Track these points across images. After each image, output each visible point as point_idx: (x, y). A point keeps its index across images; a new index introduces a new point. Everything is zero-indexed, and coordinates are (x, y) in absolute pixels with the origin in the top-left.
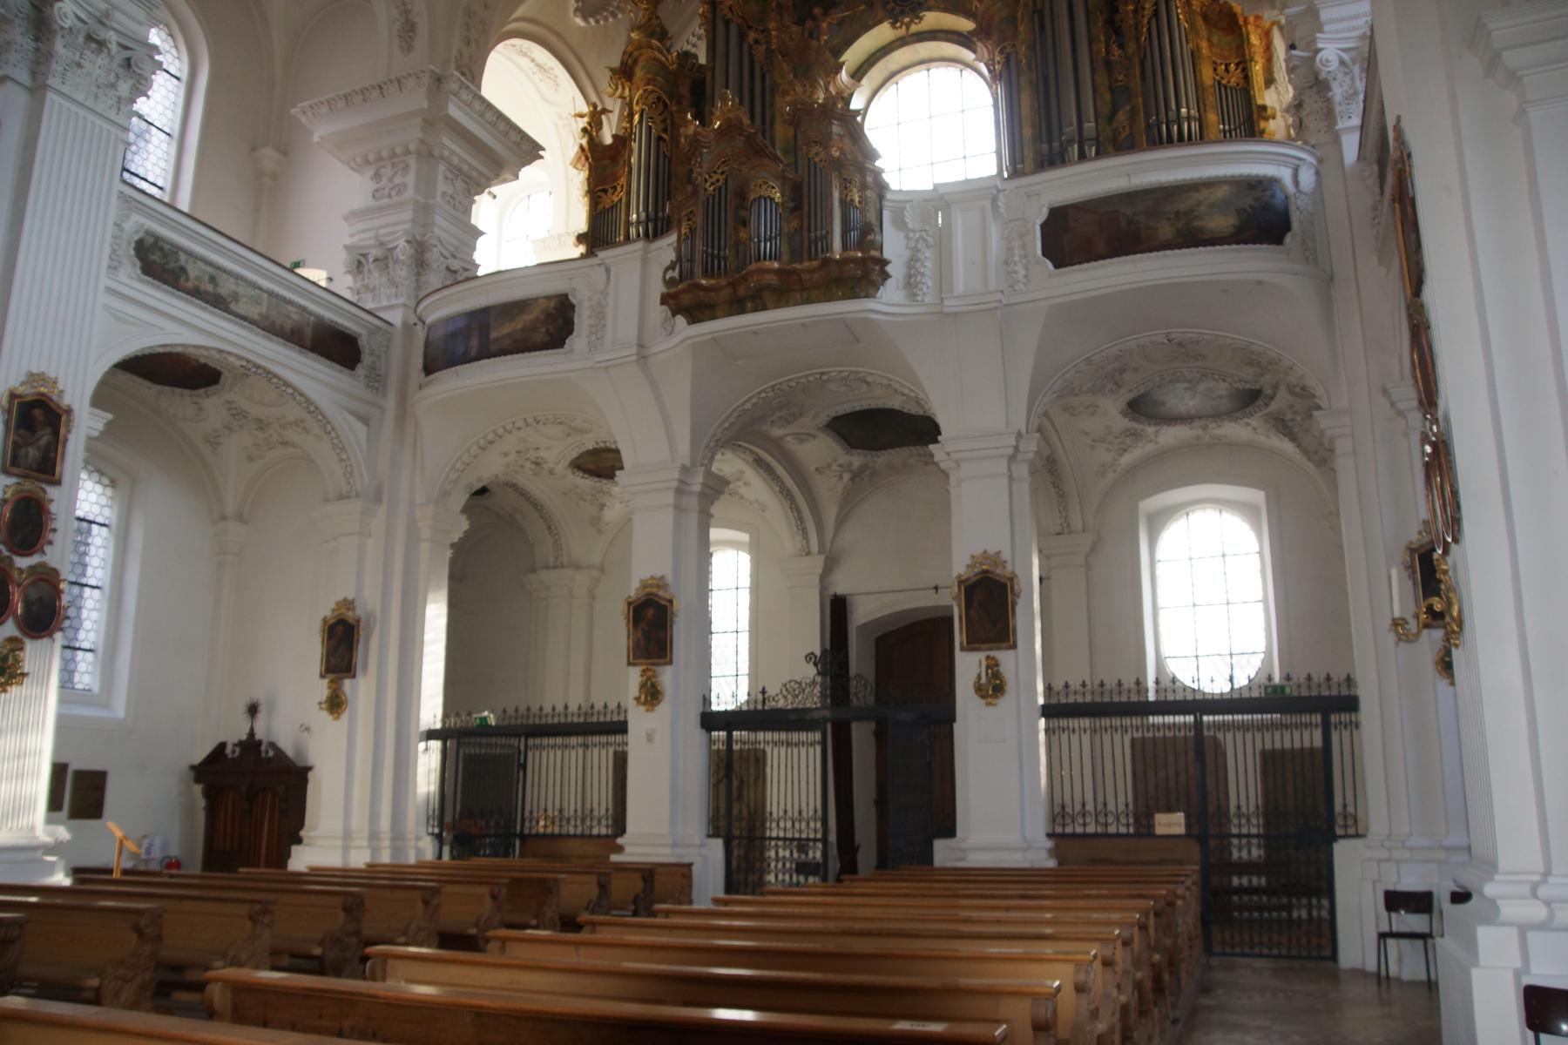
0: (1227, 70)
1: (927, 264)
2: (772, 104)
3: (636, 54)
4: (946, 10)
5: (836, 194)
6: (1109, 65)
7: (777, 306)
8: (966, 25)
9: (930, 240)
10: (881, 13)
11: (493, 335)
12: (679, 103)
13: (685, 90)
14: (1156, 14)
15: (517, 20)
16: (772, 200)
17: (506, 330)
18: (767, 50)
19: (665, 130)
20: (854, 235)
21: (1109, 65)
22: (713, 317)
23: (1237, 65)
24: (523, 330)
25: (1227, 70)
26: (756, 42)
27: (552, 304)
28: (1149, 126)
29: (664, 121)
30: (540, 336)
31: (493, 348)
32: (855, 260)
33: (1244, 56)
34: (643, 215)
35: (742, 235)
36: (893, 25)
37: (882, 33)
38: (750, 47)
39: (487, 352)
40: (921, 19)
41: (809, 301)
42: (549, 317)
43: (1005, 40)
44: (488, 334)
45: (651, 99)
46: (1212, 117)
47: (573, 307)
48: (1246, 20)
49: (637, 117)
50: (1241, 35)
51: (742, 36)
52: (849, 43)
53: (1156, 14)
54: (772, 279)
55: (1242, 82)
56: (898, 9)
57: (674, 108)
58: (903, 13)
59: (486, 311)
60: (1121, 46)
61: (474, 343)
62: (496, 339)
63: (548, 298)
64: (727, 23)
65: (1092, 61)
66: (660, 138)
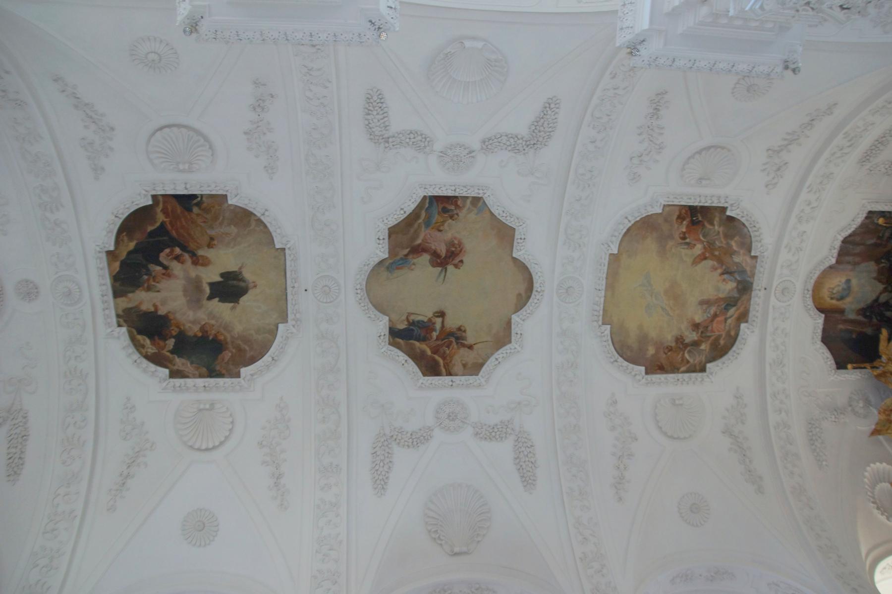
15: (867, 554)
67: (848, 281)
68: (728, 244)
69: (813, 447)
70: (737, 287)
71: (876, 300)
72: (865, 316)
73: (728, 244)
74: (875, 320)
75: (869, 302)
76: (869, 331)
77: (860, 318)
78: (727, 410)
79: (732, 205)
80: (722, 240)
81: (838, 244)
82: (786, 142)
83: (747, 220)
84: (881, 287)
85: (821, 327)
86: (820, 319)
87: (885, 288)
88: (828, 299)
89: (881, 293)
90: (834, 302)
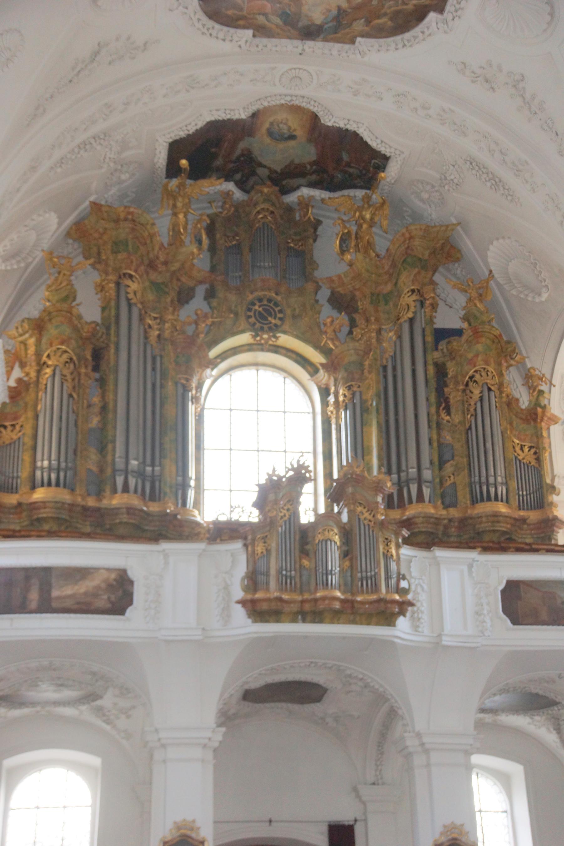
0: (522, 449)
1: (425, 604)
2: (162, 386)
3: (54, 314)
4: (297, 337)
5: (381, 547)
6: (439, 426)
7: (332, 622)
8: (317, 358)
9: (425, 587)
10: (243, 323)
11: (55, 593)
12: (86, 367)
13: (88, 355)
14: (481, 399)
16: (335, 543)
17: (68, 591)
18: (159, 336)
19: (74, 388)
20: (393, 581)
21: (439, 426)
22: (278, 621)
23: (531, 448)
24: (86, 594)
25: (522, 449)
26: (150, 327)
27: (113, 576)
28: (471, 484)
29: (73, 379)
30: (102, 602)
31: (54, 605)
32: (394, 602)
33: (538, 443)
34: (54, 463)
35: (305, 562)
36: (254, 337)
37: (245, 338)
38: (145, 329)
39: (46, 606)
40: (277, 338)
41: (353, 622)
42: (110, 587)
43: (353, 380)
44: (49, 592)
45: (65, 357)
46: (513, 484)
47: (132, 583)
48: (542, 420)
49: (48, 371)
50: (536, 427)
51: (141, 319)
52: (215, 342)
53: (481, 399)
54: (337, 605)
55: (533, 463)
56: (258, 325)
57: (83, 370)
58: (262, 329)
59: (47, 570)
60: (449, 413)
61: (34, 596)
62: (58, 598)
63: (108, 570)
64: (130, 305)
65: (429, 421)
66: (70, 396)
67: (292, 137)
68: (385, 14)
69: (76, 150)
70: (313, 24)
71: (260, 165)
72: (240, 156)
73: (385, 14)
74: (231, 165)
75: (260, 159)
76: (219, 162)
77: (238, 152)
78: (129, 38)
79: (446, 22)
80: (393, 9)
81: (352, 127)
82: (528, 96)
83: (415, 37)
84: (278, 169)
85: (236, 117)
86: (243, 115)
87: (276, 172)
88: (271, 119)
89: (269, 169)
90: (267, 125)
